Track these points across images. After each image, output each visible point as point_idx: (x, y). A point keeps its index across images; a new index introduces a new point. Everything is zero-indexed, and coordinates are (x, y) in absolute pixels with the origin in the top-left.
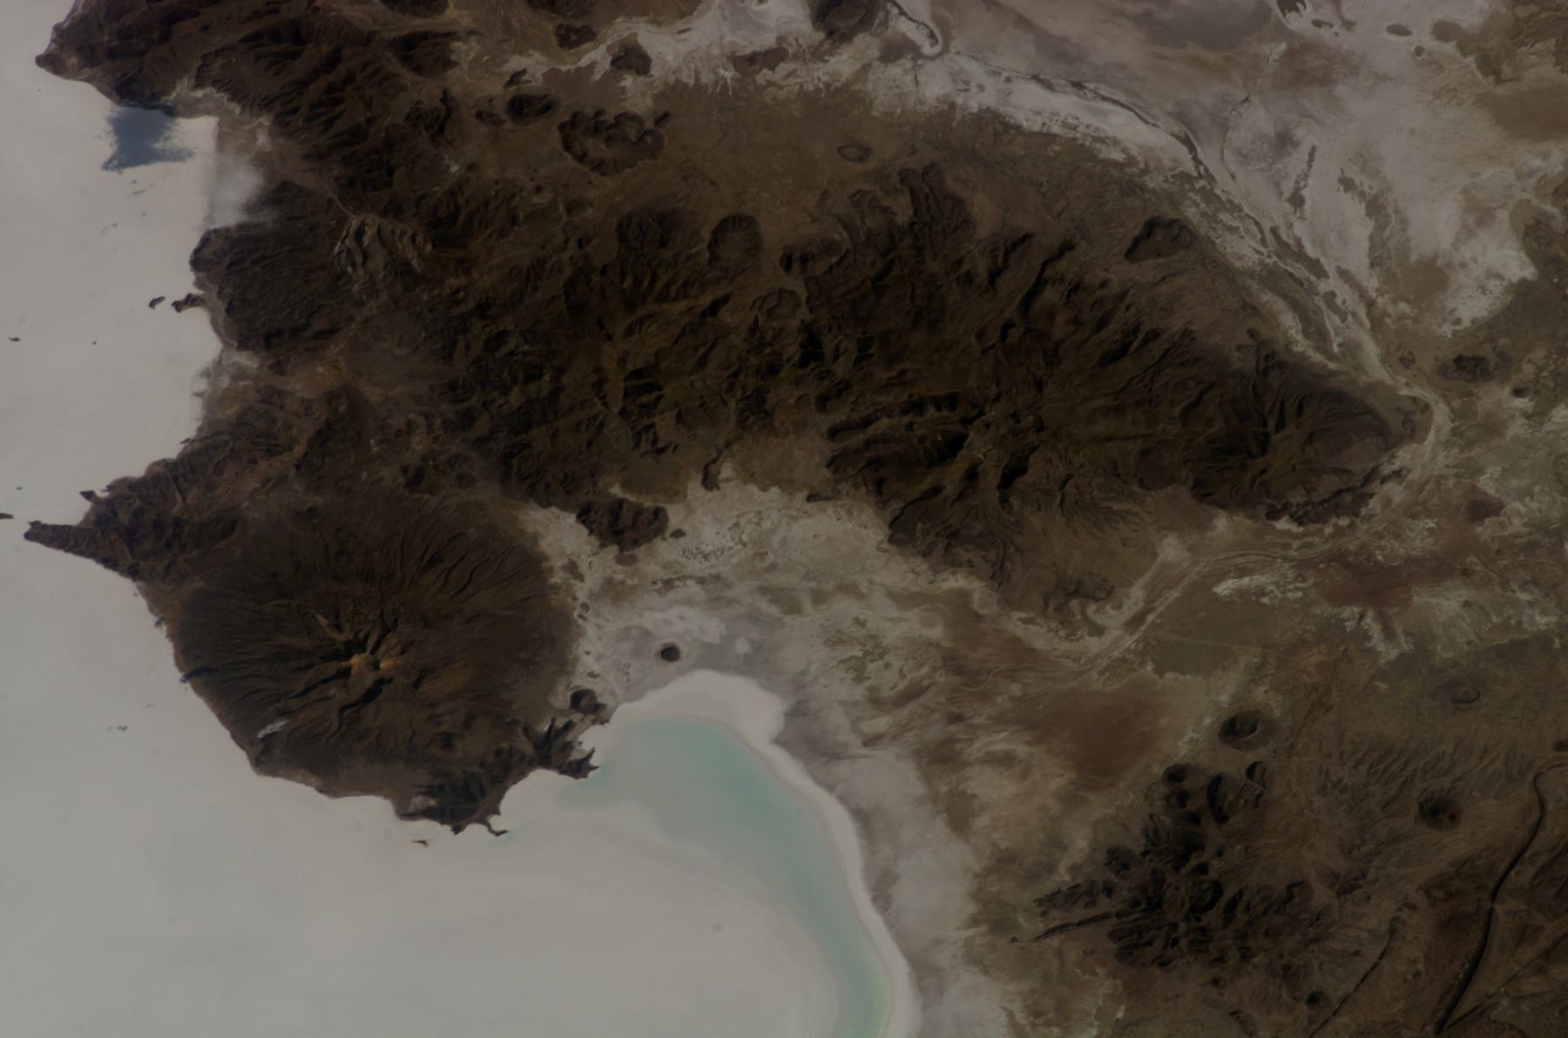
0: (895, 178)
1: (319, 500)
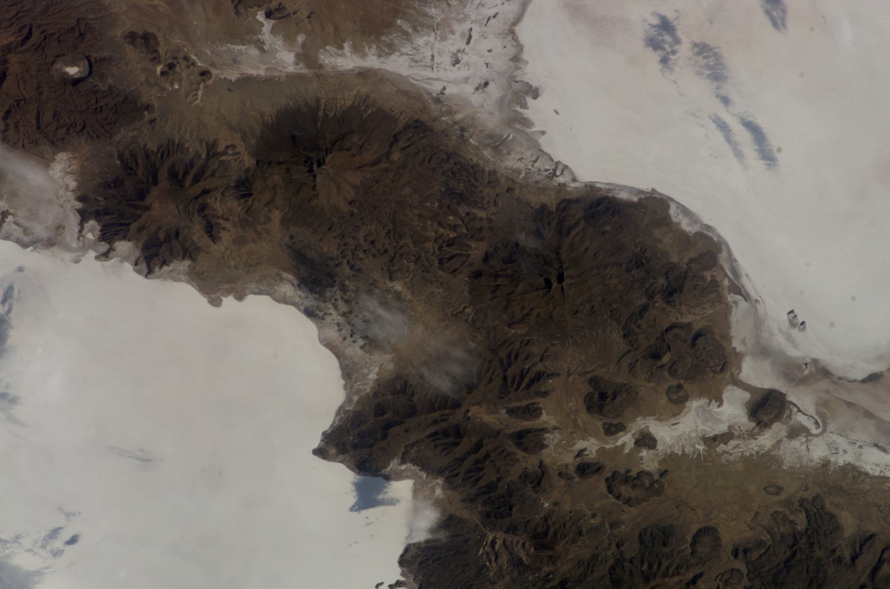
0: (797, 504)
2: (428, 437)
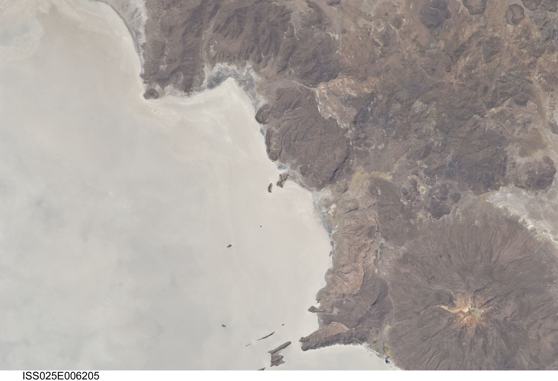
1: (403, 248)
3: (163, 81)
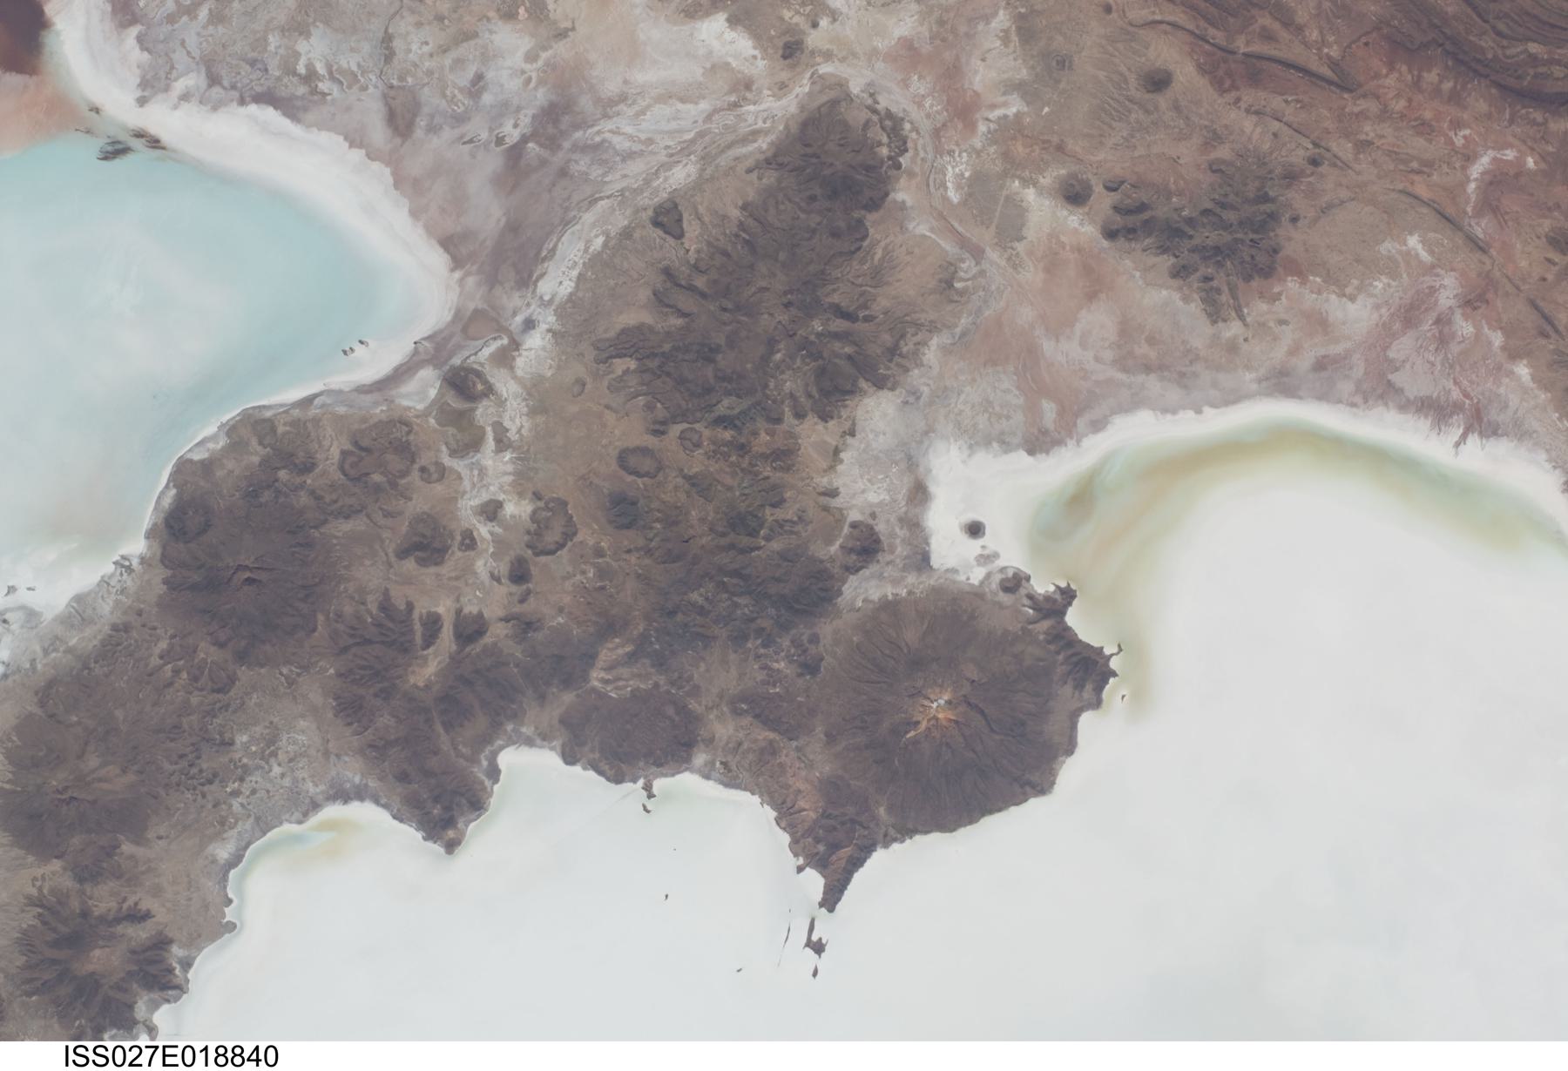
2: (447, 732)
3: (449, 822)
